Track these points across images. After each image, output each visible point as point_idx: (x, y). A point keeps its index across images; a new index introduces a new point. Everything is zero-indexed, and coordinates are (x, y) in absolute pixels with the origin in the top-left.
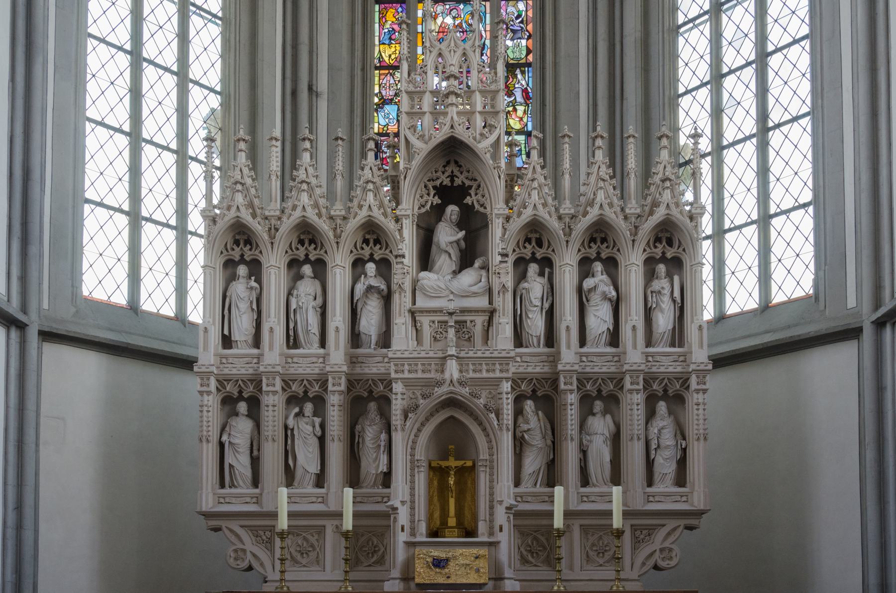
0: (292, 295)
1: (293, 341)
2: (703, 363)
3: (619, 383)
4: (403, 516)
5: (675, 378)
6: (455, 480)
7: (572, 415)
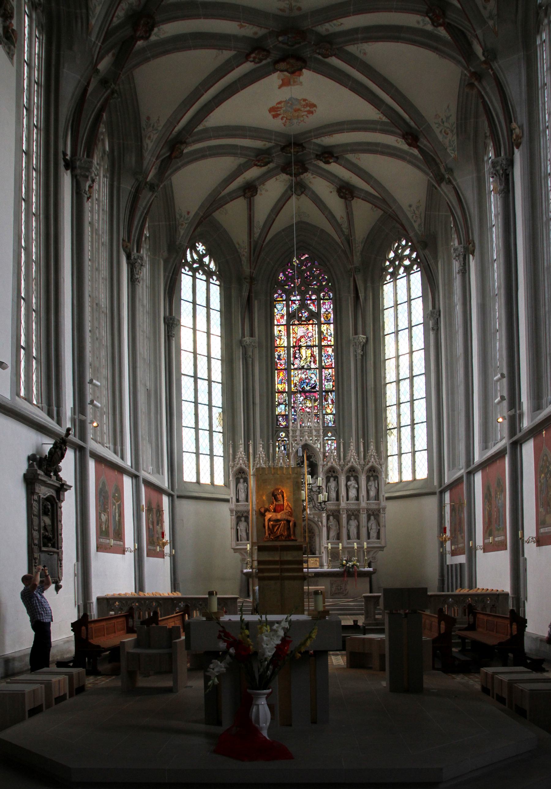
3: (359, 511)
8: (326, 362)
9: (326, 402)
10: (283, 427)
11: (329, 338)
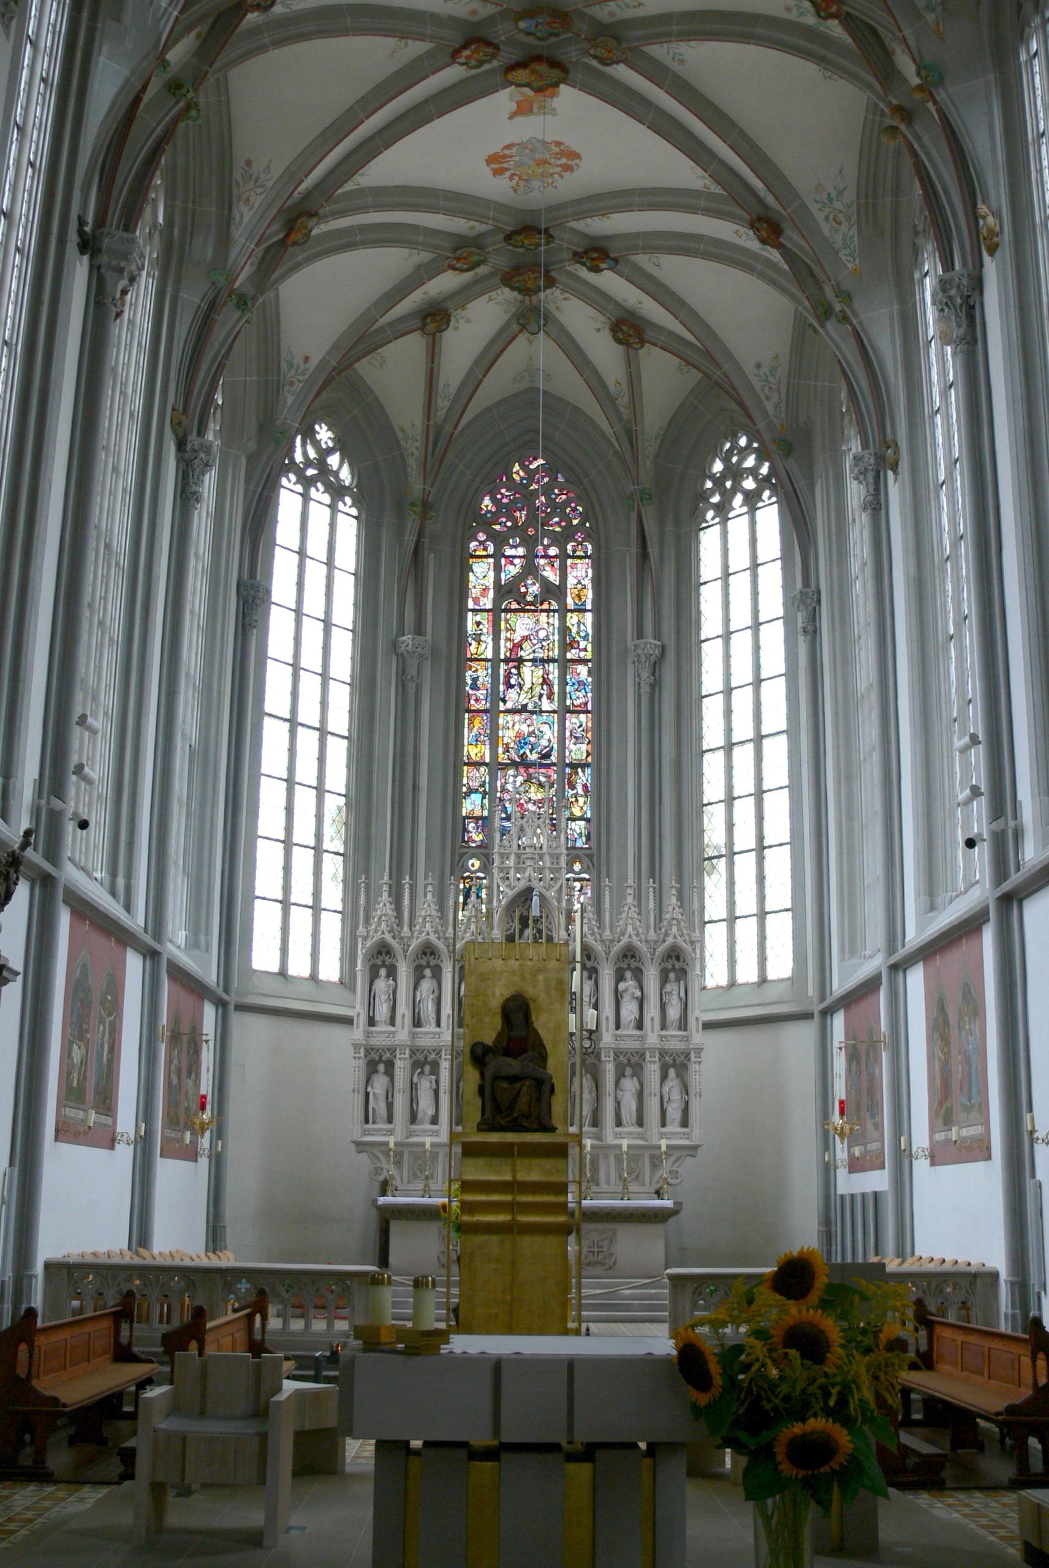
1: (417, 1022)
3: (642, 1056)
8: (574, 697)
9: (573, 790)
10: (477, 847)
11: (583, 644)
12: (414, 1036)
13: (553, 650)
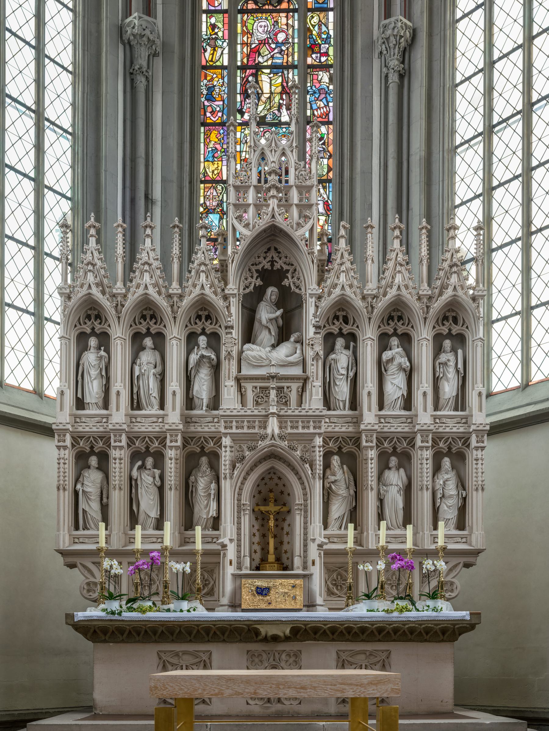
0: (136, 364)
2: (482, 424)
3: (411, 442)
4: (231, 553)
5: (458, 438)
6: (274, 523)
7: (371, 468)
12: (132, 419)
13: (293, 55)
